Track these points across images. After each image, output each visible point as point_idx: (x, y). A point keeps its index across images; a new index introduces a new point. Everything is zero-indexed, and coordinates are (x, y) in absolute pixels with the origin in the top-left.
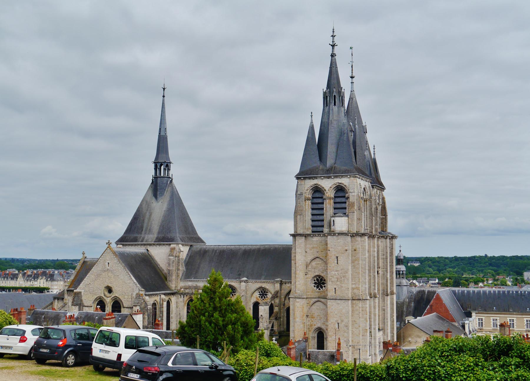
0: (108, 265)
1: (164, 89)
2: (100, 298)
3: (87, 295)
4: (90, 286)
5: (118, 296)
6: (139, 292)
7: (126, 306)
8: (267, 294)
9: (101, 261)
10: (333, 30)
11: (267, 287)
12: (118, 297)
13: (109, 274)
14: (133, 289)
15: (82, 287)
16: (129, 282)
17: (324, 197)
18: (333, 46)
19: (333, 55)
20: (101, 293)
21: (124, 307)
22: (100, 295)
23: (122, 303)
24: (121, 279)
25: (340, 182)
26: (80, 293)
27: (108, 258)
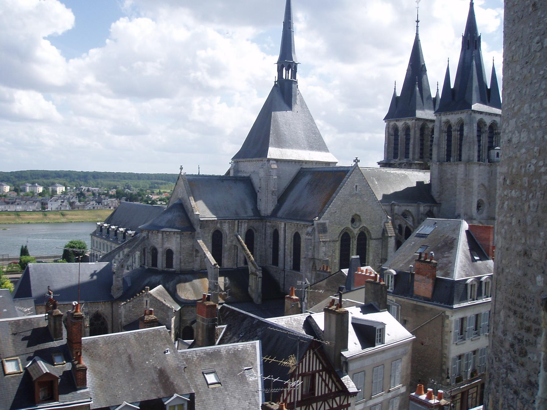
0: (355, 189)
2: (347, 228)
3: (331, 226)
4: (336, 215)
5: (366, 226)
6: (387, 220)
7: (374, 238)
8: (407, 216)
9: (349, 184)
11: (410, 210)
12: (366, 228)
13: (358, 200)
14: (381, 217)
15: (326, 216)
16: (377, 208)
17: (482, 130)
20: (349, 223)
21: (371, 239)
22: (347, 226)
23: (370, 233)
24: (370, 206)
25: (495, 119)
26: (325, 224)
27: (356, 180)
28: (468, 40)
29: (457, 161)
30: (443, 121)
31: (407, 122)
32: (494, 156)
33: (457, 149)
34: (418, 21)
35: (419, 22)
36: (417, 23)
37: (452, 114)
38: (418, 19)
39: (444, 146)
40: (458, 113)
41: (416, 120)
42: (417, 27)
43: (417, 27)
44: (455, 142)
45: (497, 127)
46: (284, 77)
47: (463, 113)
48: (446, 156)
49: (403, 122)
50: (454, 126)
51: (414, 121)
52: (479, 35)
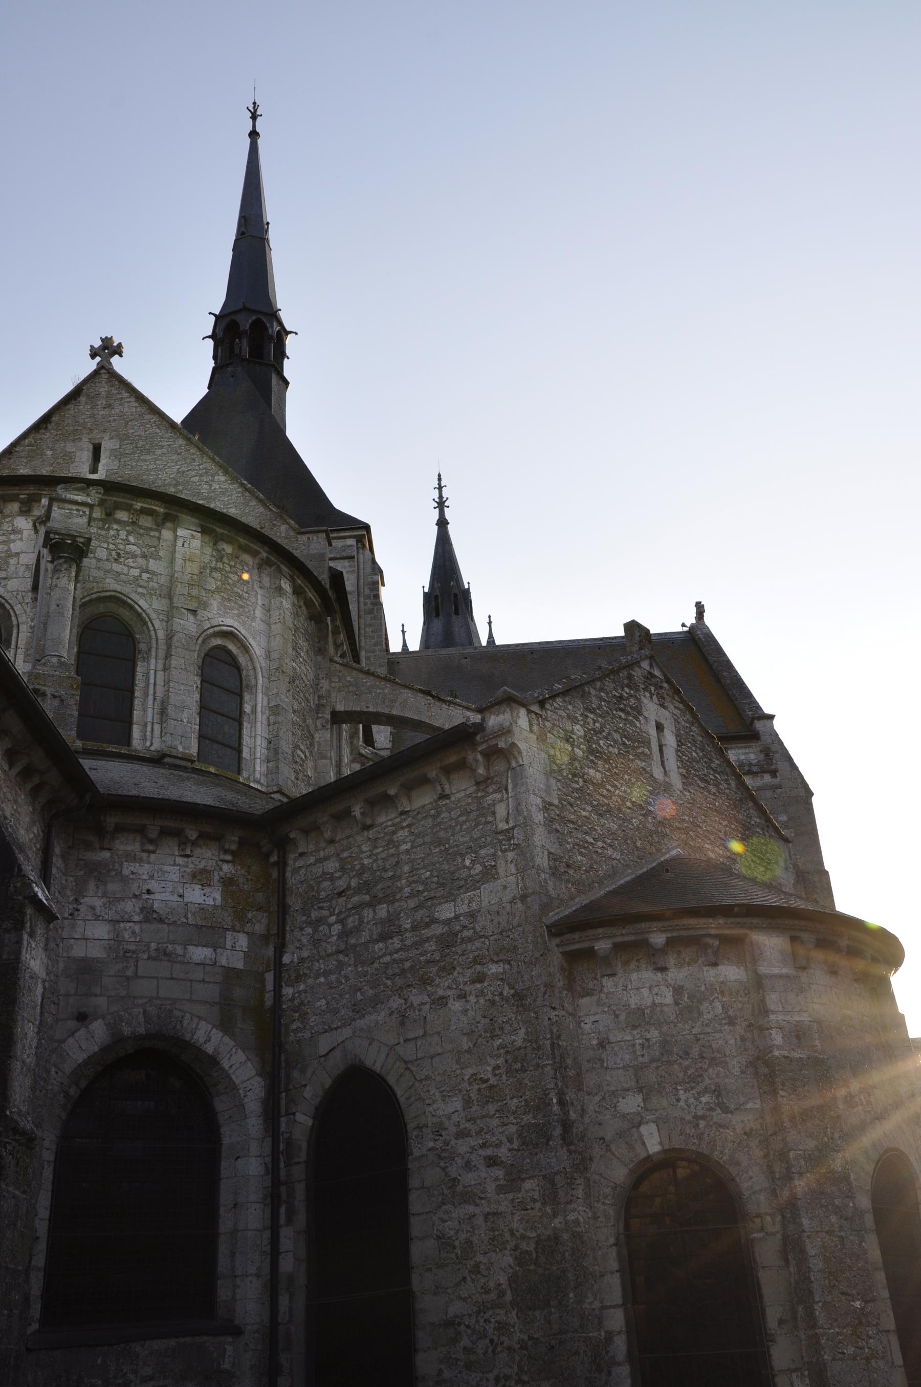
10: (439, 475)
19: (442, 523)
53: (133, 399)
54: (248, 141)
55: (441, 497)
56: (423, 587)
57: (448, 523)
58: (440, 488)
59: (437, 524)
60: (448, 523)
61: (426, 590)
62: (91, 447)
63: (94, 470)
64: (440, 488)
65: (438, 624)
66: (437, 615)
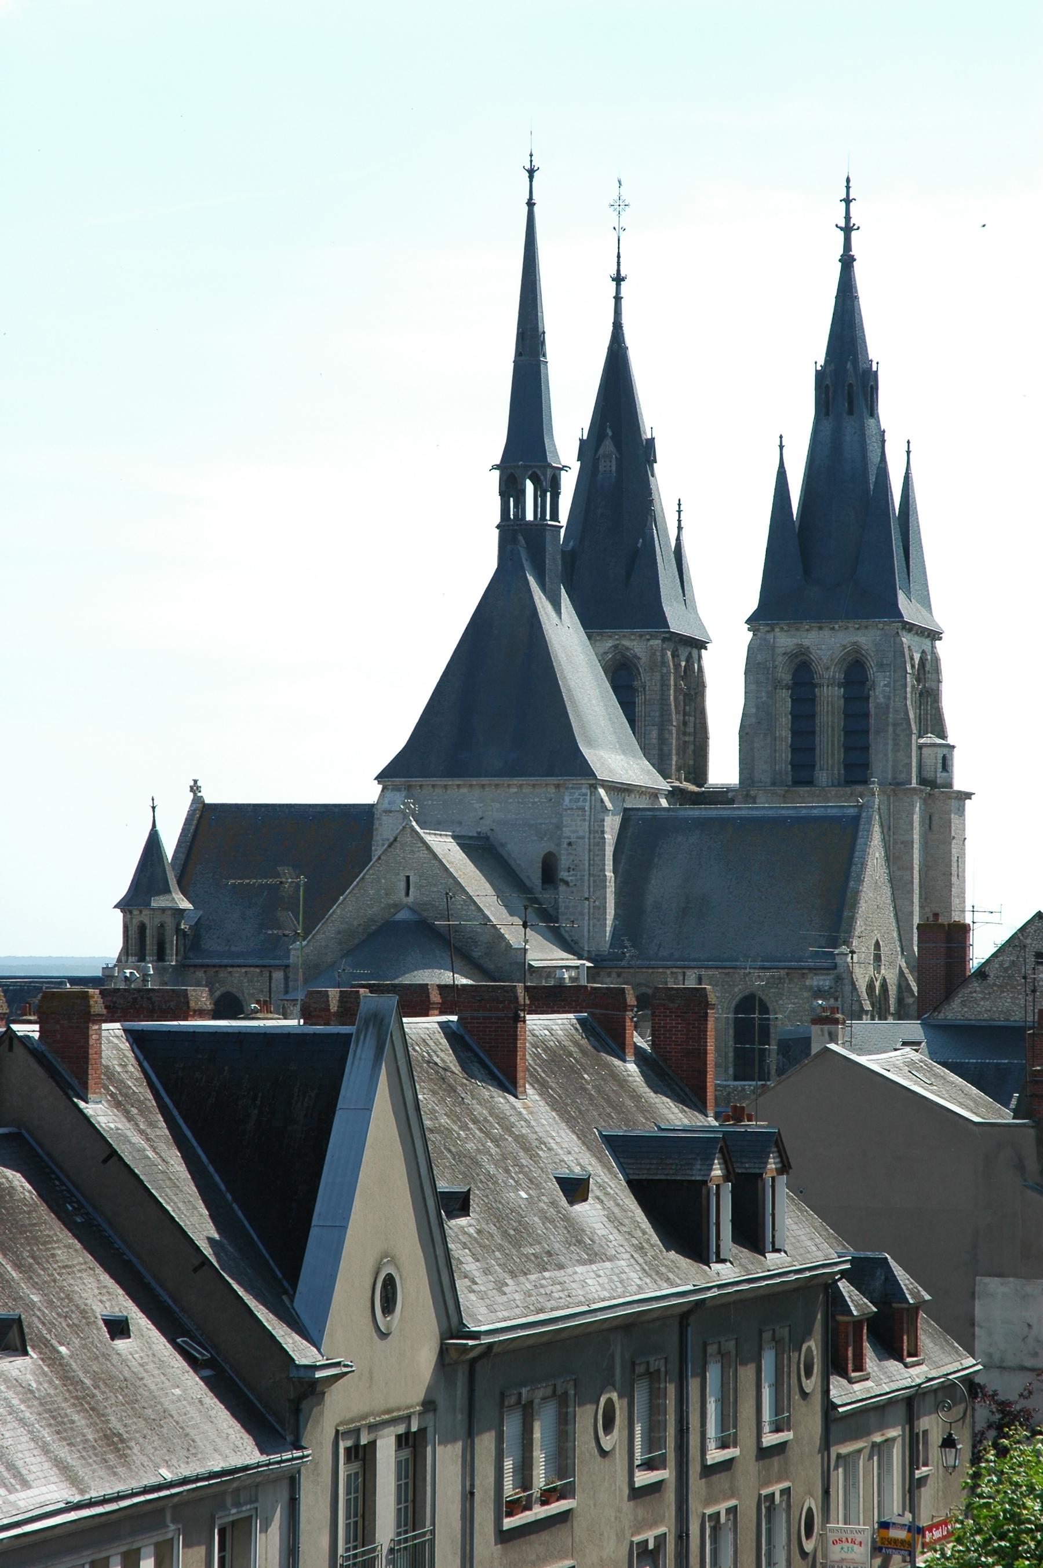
1: (531, 172)
10: (848, 180)
18: (848, 230)
19: (847, 262)
28: (851, 385)
29: (839, 785)
30: (781, 650)
31: (626, 643)
32: (936, 768)
33: (839, 741)
34: (618, 279)
35: (623, 279)
36: (618, 286)
37: (821, 628)
38: (618, 271)
39: (784, 734)
40: (847, 628)
41: (664, 640)
42: (618, 299)
43: (618, 299)
44: (833, 722)
45: (924, 671)
46: (548, 517)
47: (866, 627)
48: (790, 766)
49: (610, 643)
50: (828, 669)
51: (658, 642)
52: (874, 368)
53: (424, 848)
54: (526, 208)
55: (848, 218)
56: (816, 363)
57: (855, 260)
58: (848, 201)
59: (840, 260)
60: (855, 260)
61: (819, 368)
62: (405, 878)
63: (407, 894)
64: (848, 201)
65: (827, 426)
66: (827, 414)
